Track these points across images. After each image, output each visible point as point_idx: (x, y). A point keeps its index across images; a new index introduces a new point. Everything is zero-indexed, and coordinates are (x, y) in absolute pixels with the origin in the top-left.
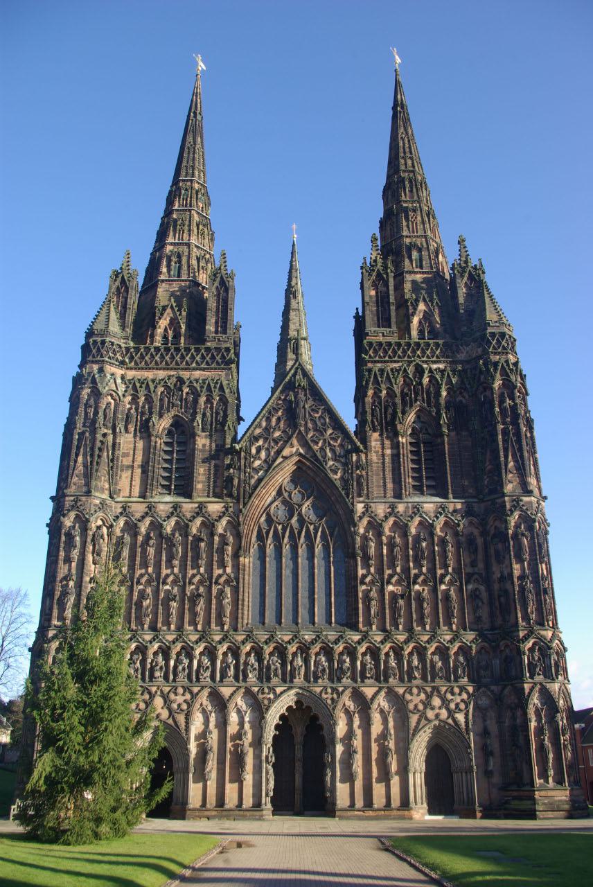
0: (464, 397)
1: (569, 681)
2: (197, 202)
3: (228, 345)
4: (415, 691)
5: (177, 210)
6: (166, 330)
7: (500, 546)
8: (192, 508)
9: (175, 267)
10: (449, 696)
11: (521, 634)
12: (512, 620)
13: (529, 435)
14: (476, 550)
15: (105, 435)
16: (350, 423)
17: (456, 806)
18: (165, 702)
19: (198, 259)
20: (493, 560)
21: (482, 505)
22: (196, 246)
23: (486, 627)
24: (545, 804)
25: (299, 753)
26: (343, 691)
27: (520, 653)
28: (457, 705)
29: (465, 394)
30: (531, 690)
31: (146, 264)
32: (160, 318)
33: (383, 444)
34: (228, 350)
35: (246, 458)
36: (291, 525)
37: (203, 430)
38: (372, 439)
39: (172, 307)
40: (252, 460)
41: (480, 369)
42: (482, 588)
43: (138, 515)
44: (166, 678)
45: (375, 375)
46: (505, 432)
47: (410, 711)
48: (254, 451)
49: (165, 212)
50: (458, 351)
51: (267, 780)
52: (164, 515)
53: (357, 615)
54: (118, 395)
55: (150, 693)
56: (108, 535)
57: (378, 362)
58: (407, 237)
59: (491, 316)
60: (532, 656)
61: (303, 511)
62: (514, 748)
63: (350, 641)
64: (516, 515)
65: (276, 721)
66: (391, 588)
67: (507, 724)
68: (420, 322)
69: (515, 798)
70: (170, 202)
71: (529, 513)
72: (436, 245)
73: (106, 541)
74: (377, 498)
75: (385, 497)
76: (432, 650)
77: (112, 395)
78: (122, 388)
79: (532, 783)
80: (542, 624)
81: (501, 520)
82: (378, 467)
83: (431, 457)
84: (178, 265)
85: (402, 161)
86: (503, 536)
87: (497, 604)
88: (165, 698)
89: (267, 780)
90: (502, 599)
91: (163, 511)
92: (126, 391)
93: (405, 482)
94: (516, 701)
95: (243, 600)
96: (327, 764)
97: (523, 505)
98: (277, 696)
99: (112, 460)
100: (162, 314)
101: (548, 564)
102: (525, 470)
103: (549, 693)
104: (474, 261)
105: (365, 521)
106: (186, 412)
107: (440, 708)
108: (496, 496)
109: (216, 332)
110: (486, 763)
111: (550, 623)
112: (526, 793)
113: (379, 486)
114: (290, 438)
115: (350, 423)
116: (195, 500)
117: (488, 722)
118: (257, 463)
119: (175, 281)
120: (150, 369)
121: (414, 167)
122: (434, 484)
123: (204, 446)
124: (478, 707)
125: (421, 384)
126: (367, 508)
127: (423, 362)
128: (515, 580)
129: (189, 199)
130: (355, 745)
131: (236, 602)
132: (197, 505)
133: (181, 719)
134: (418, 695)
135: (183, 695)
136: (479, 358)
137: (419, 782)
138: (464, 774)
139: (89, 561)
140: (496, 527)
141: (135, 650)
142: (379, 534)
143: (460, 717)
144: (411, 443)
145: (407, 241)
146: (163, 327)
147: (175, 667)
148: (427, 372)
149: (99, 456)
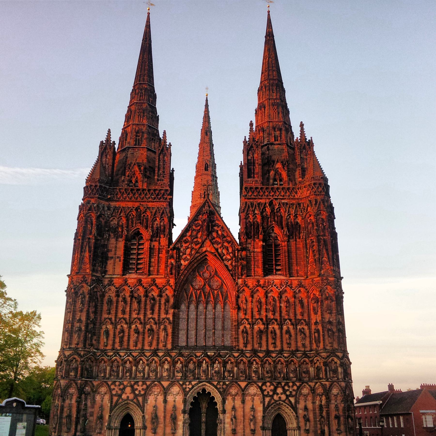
1: (352, 381)
5: (137, 103)
8: (147, 281)
9: (136, 139)
10: (286, 388)
12: (321, 345)
15: (98, 240)
20: (312, 313)
22: (149, 126)
23: (308, 349)
28: (291, 392)
31: (120, 135)
40: (181, 254)
42: (306, 327)
43: (117, 285)
48: (182, 249)
49: (130, 103)
55: (123, 384)
70: (132, 98)
87: (313, 337)
88: (132, 386)
91: (131, 283)
94: (322, 391)
98: (193, 387)
104: (308, 138)
107: (282, 394)
108: (314, 276)
110: (306, 424)
114: (203, 243)
118: (184, 257)
119: (136, 148)
132: (150, 280)
133: (140, 399)
134: (270, 386)
135: (142, 386)
138: (293, 431)
143: (292, 400)
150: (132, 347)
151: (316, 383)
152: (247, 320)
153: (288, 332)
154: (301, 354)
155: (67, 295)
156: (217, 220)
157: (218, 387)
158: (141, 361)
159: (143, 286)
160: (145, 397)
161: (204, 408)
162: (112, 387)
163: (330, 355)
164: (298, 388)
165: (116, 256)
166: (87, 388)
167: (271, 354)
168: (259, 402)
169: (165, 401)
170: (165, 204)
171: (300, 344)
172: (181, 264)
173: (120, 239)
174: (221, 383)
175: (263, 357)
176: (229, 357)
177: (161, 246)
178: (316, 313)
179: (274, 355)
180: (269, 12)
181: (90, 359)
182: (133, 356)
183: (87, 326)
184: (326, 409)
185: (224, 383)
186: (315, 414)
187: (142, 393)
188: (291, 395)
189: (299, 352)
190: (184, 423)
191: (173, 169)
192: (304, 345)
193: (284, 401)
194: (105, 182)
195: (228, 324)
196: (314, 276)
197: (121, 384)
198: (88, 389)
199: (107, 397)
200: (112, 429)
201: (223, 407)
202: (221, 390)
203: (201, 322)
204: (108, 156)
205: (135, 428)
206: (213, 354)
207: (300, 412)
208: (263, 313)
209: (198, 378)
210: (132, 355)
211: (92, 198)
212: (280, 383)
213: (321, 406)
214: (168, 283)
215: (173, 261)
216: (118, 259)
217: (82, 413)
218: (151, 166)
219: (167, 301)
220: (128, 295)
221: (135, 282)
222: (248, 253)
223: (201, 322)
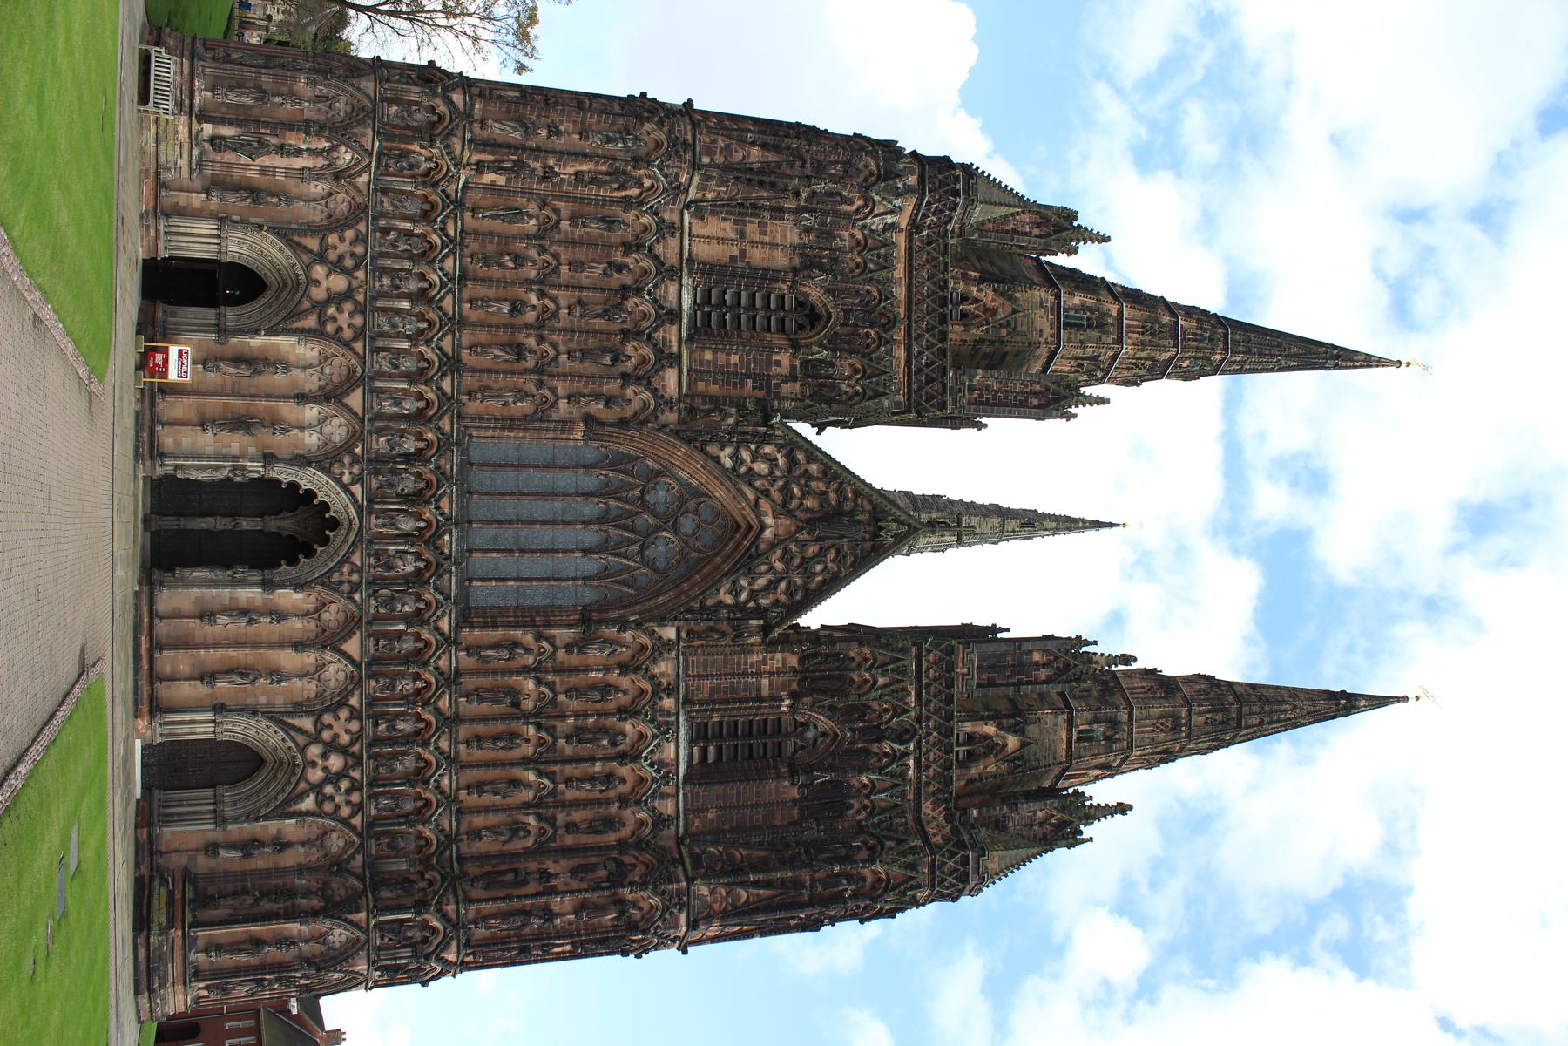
0: (858, 812)
2: (1189, 358)
3: (949, 407)
4: (354, 726)
6: (976, 301)
7: (602, 873)
8: (671, 342)
9: (1082, 318)
10: (344, 784)
11: (450, 908)
12: (477, 893)
13: (792, 923)
14: (597, 832)
15: (797, 194)
16: (813, 619)
17: (157, 793)
18: (339, 294)
19: (1095, 358)
20: (577, 861)
21: (672, 844)
22: (1115, 356)
23: (465, 850)
24: (160, 947)
25: (245, 524)
26: (355, 602)
27: (421, 906)
28: (332, 798)
29: (863, 814)
30: (356, 925)
31: (1086, 269)
32: (995, 291)
33: (778, 673)
34: (943, 406)
35: (754, 435)
36: (638, 513)
37: (805, 363)
38: (787, 654)
39: (1015, 311)
40: (753, 447)
41: (905, 840)
42: (529, 842)
43: (659, 249)
44: (382, 295)
45: (899, 660)
46: (798, 884)
47: (319, 717)
48: (768, 449)
49: (1174, 303)
50: (937, 803)
51: (204, 468)
52: (660, 292)
53: (485, 626)
54: (866, 217)
55: (356, 267)
56: (625, 197)
57: (919, 665)
58: (1131, 715)
59: (993, 860)
60: (413, 927)
61: (665, 534)
62: (257, 893)
63: (439, 613)
64: (655, 901)
65: (305, 485)
66: (530, 685)
67: (297, 881)
68: (986, 737)
69: (171, 894)
70: (1190, 311)
71: (659, 923)
72: (1115, 764)
73: (615, 194)
74: (686, 661)
75: (687, 675)
76: (426, 755)
77: (865, 206)
78: (876, 224)
79: (196, 924)
80: (468, 944)
81: (646, 875)
82: (739, 664)
83: (755, 756)
84: (1085, 323)
85: (1255, 709)
86: (618, 878)
87: (503, 867)
88: (348, 294)
89: (204, 468)
90: (510, 877)
91: (666, 292)
92: (872, 231)
93: (713, 710)
94: (338, 899)
95: (511, 429)
96: (229, 572)
97: (672, 913)
98: (346, 488)
99: (754, 206)
100: (1002, 295)
101: (573, 956)
102: (734, 915)
103: (352, 956)
104: (1087, 831)
105: (645, 640)
106: (836, 333)
107: (325, 769)
108: (689, 867)
109: (971, 389)
111: (471, 958)
112: (179, 915)
113: (705, 663)
114: (790, 514)
115: (813, 619)
116: (684, 347)
117: (301, 850)
118: (746, 455)
120: (910, 272)
121: (1247, 727)
122: (710, 760)
123: (778, 363)
124: (326, 833)
125: (879, 740)
126: (668, 645)
127: (919, 742)
128: (544, 900)
129: (1195, 343)
130: (261, 619)
131: (508, 422)
132: (675, 349)
133: (311, 322)
134: (347, 731)
136: (926, 840)
137: (198, 730)
138: (212, 807)
139: (582, 164)
140: (634, 866)
141: (429, 242)
142: (624, 668)
143: (309, 803)
144: (779, 720)
145: (1123, 716)
146: (981, 296)
147: (398, 311)
148: (902, 748)
149: (761, 184)
150: (470, 290)
151: (362, 879)
152: (553, 656)
153: (515, 783)
154: (447, 828)
155: (631, 97)
156: (856, 557)
157: (346, 569)
158: (425, 325)
159: (655, 330)
160: (317, 333)
161: (278, 523)
162: (349, 234)
163: (449, 920)
164: (345, 822)
165: (748, 248)
166: (348, 156)
167: (447, 736)
168: (300, 699)
169: (303, 398)
170: (900, 398)
171: (479, 821)
172: (722, 449)
173: (797, 261)
174: (355, 577)
175: (437, 709)
176: (437, 602)
177: (777, 385)
178: (574, 872)
179: (444, 744)
180: (1405, 699)
181: (436, 167)
182: (442, 299)
183: (538, 151)
184: (282, 912)
185: (355, 587)
186: (267, 873)
187: (330, 328)
188: (322, 799)
189: (454, 824)
190: (235, 458)
191: (985, 426)
192: (476, 834)
193: (302, 776)
194: (965, 220)
195: (537, 595)
196: (689, 867)
197: (359, 262)
198: (345, 157)
199: (316, 215)
200: (219, 237)
201: (283, 586)
202: (336, 577)
203: (542, 509)
204: (1036, 232)
205: (222, 308)
206: (446, 551)
207: (272, 827)
208: (574, 704)
209: (370, 501)
210: (446, 293)
211: (921, 180)
212: (358, 761)
213: (291, 893)
214: (666, 403)
215: (731, 421)
216: (735, 252)
217: (273, 141)
218: (1007, 358)
219: (609, 401)
220: (627, 279)
221: (668, 305)
222: (755, 658)
223: (542, 509)
